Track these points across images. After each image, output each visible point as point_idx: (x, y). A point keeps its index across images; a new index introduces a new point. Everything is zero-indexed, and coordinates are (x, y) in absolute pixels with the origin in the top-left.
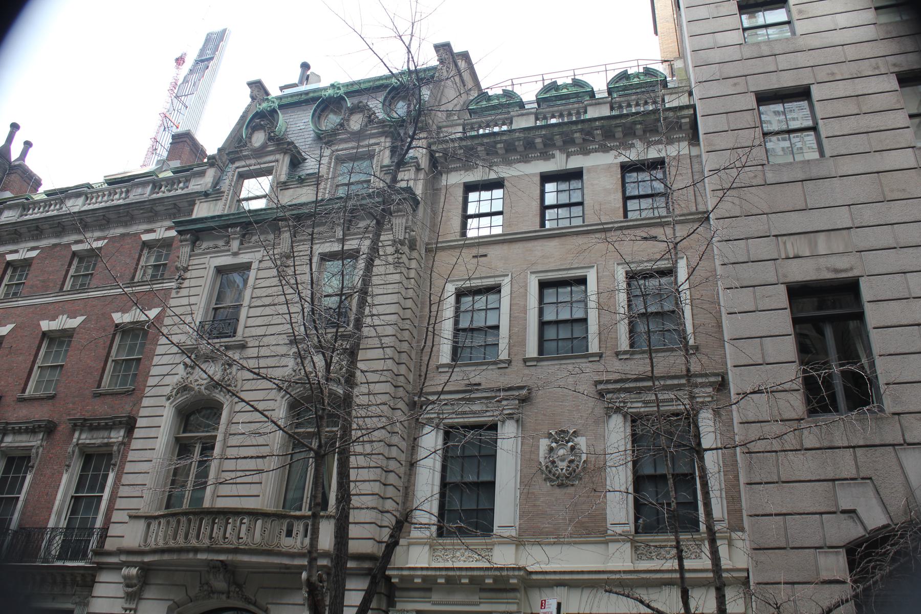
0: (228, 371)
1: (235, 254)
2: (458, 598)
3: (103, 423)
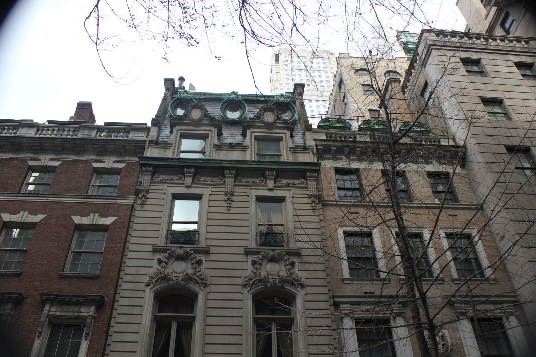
0: (198, 269)
1: (188, 187)
3: (74, 299)
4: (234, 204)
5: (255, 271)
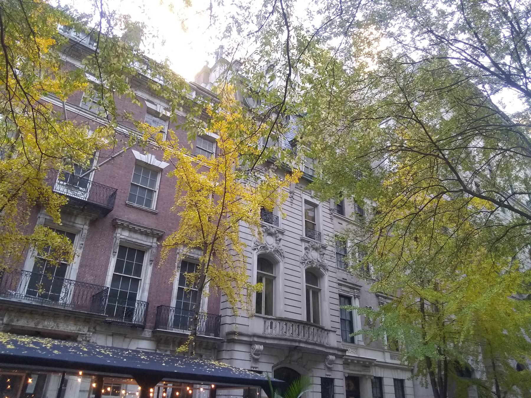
2: (356, 369)
4: (294, 202)
5: (307, 254)
